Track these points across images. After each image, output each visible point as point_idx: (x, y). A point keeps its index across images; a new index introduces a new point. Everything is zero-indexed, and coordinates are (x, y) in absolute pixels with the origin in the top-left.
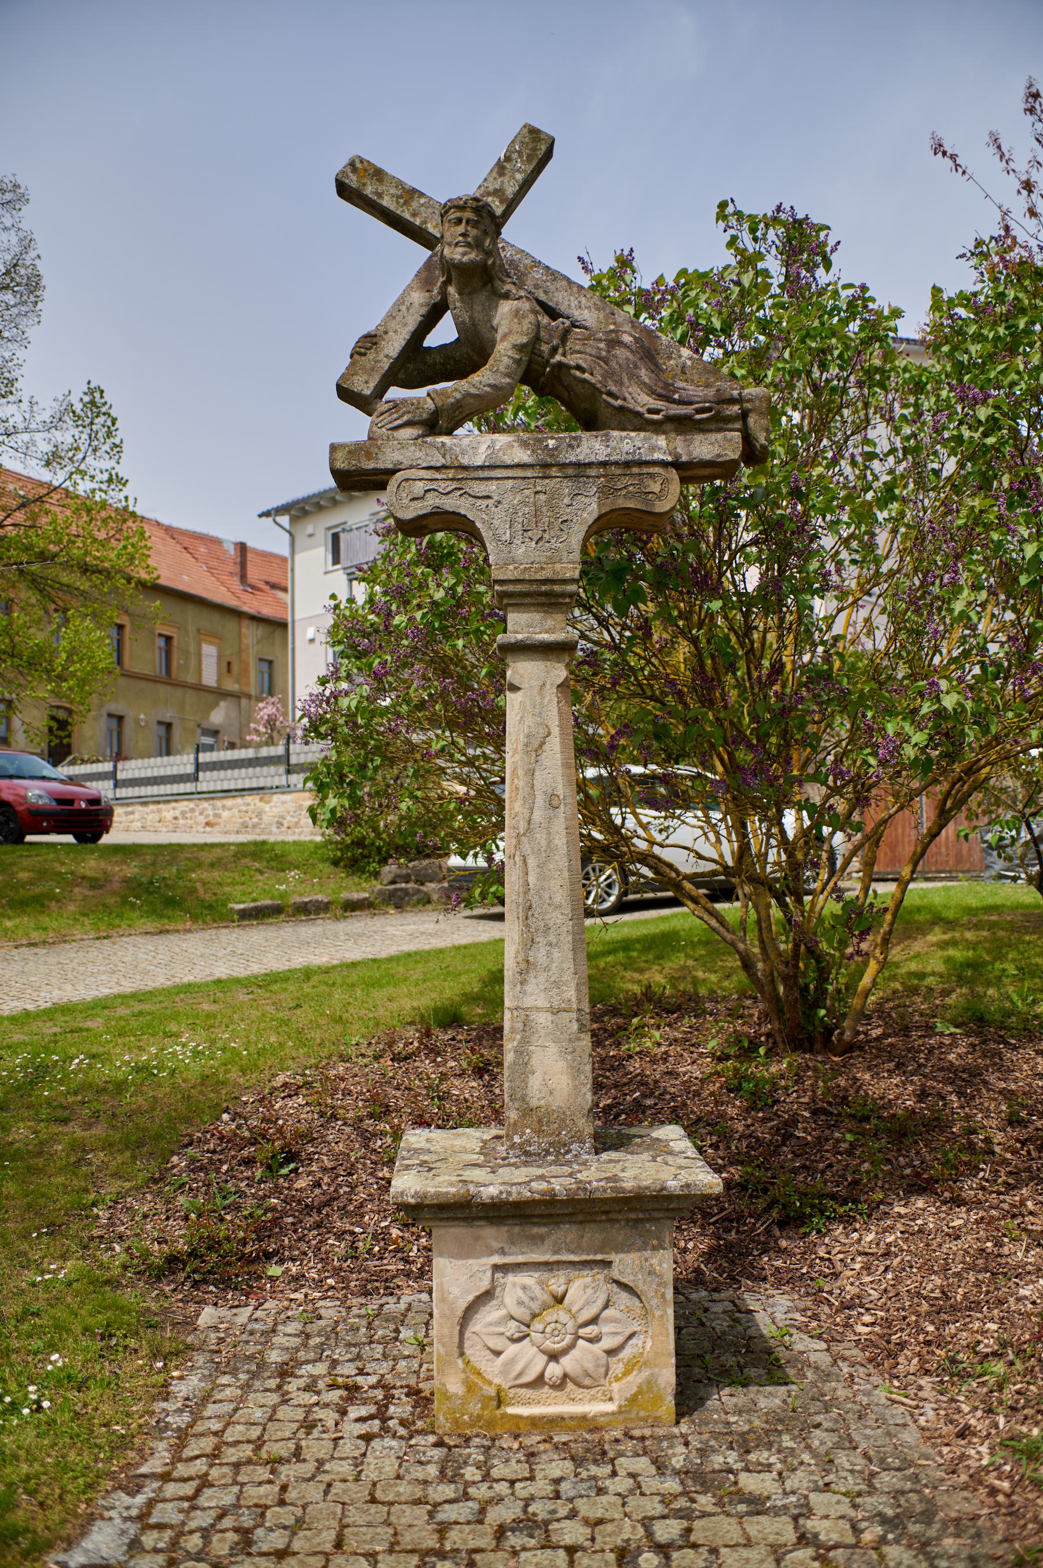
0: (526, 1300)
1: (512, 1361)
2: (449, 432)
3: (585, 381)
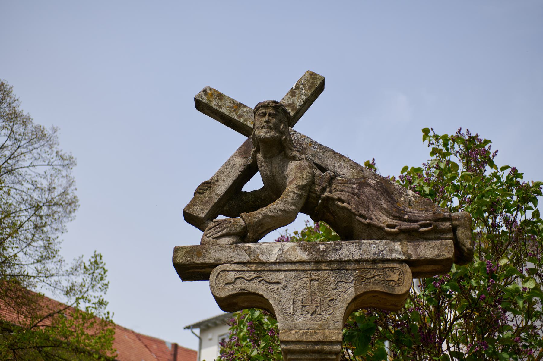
2: (255, 241)
3: (344, 208)
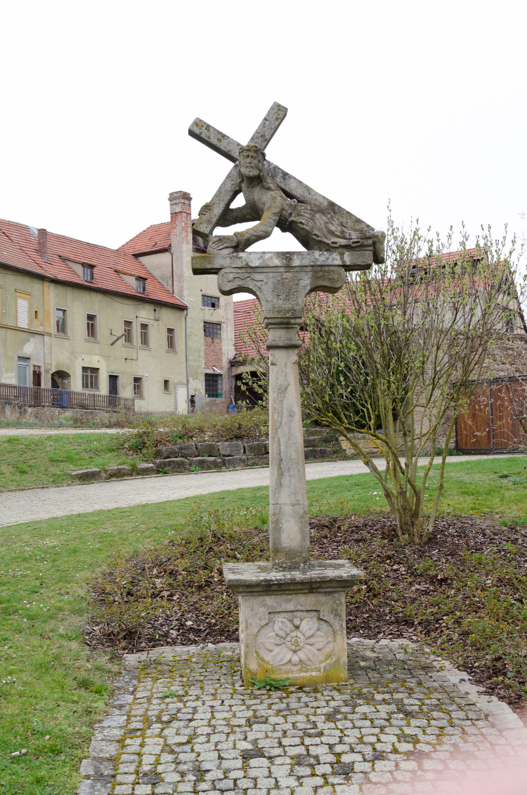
0: (283, 627)
1: (277, 654)
2: (243, 251)
3: (304, 229)
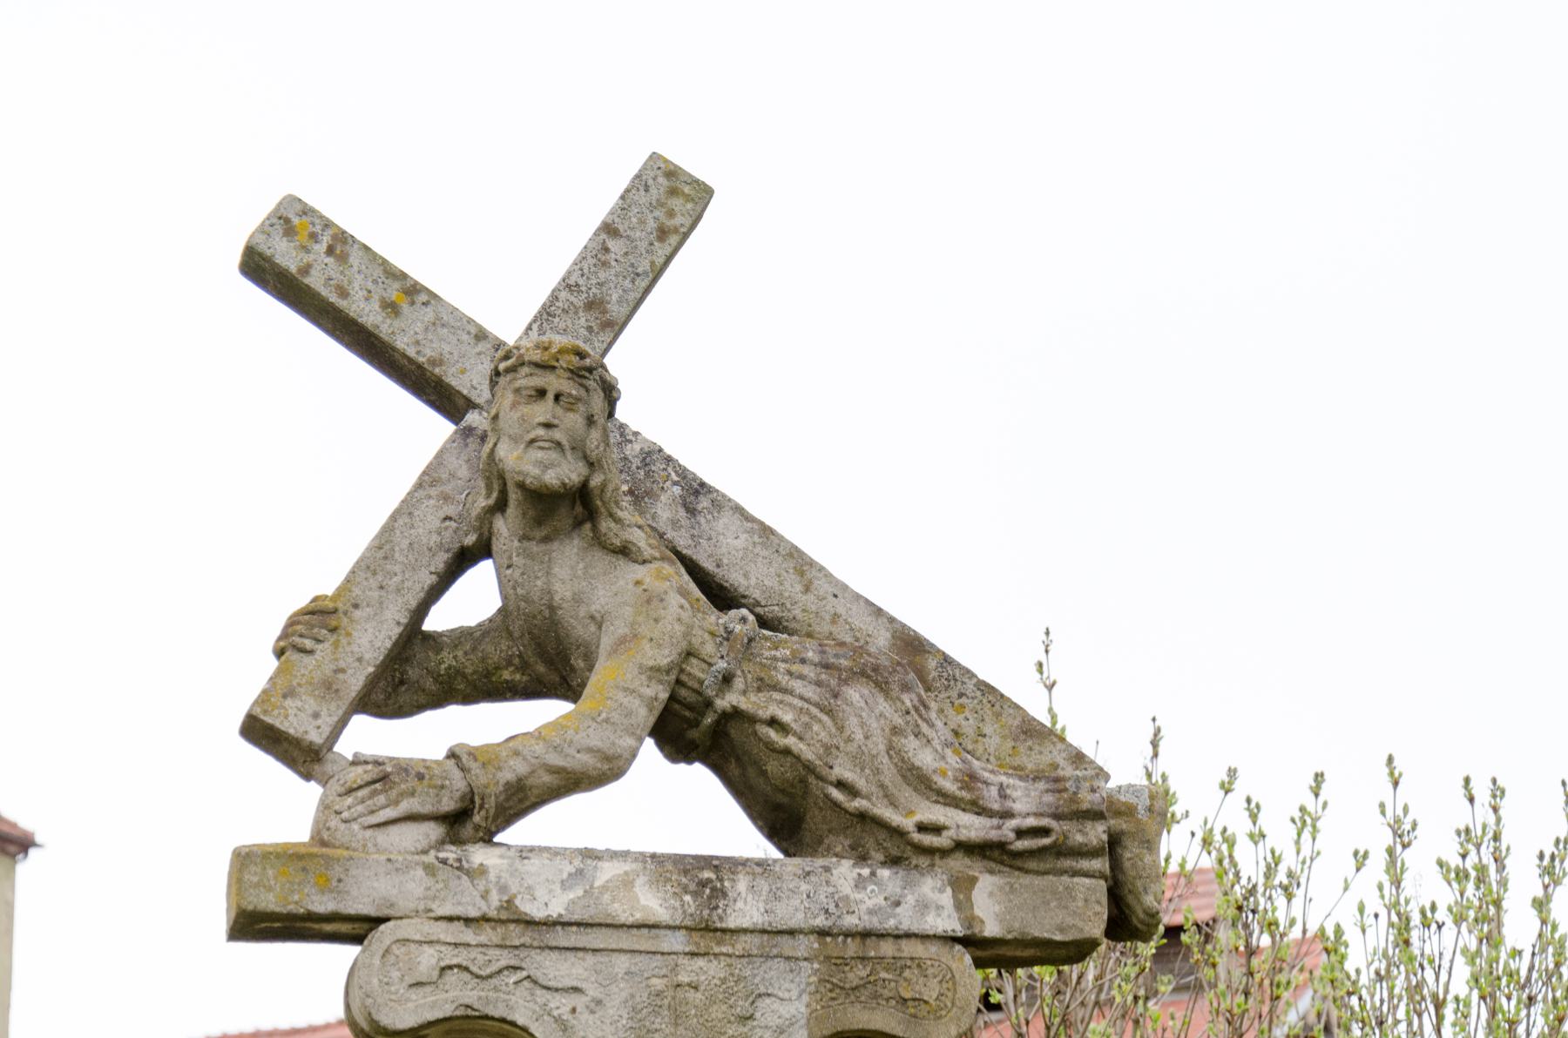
2: (488, 839)
3: (787, 752)
